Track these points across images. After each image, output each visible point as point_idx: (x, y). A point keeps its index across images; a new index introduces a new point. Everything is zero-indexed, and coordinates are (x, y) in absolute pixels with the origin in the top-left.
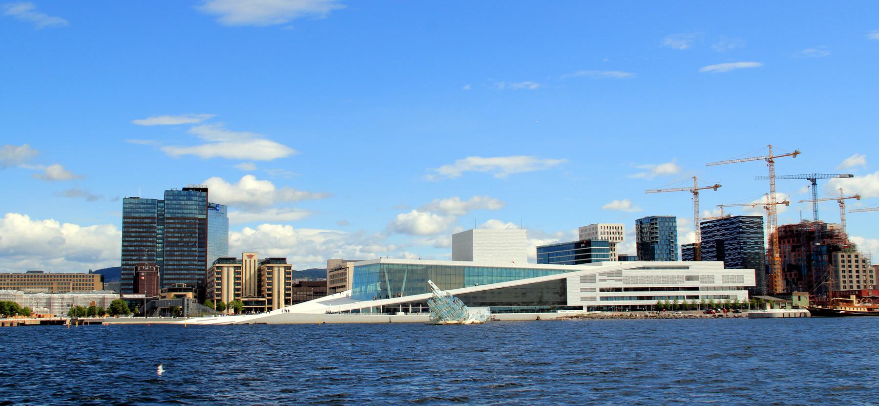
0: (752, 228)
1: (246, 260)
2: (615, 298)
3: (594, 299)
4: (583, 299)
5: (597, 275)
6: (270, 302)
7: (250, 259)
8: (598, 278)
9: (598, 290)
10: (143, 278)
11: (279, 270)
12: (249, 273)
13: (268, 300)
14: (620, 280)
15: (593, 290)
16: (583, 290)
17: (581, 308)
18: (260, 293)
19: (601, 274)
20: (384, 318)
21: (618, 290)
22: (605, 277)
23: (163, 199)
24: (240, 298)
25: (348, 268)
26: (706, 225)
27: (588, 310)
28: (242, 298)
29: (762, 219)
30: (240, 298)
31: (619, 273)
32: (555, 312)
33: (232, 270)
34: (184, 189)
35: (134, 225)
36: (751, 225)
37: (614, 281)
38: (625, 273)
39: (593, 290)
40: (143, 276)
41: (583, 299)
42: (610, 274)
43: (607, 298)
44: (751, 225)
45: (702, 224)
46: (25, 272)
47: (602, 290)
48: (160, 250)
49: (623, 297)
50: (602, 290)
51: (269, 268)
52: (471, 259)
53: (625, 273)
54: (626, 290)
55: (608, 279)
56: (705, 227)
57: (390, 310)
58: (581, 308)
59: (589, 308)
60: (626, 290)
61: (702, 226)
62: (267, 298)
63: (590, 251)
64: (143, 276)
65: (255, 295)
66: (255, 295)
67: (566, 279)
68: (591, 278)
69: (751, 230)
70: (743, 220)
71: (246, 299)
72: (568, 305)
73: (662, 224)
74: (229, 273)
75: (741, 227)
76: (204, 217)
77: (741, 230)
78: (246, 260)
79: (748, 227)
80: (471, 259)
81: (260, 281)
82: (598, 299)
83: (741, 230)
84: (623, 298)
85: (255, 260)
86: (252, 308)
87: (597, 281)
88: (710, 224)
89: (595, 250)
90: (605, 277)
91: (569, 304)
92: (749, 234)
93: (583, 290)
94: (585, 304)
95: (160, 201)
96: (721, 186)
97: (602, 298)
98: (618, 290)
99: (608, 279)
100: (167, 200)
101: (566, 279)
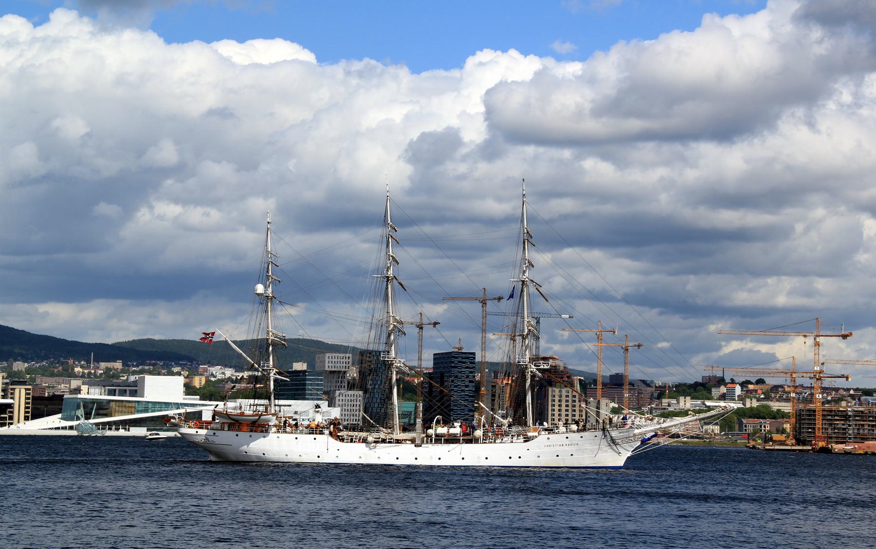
6: (11, 418)
11: (20, 391)
13: (9, 416)
36: (464, 360)
44: (464, 360)
45: (434, 355)
51: (12, 389)
52: (143, 396)
69: (463, 365)
70: (455, 356)
75: (453, 362)
77: (453, 365)
79: (460, 362)
83: (453, 365)
92: (461, 369)
96: (439, 323)
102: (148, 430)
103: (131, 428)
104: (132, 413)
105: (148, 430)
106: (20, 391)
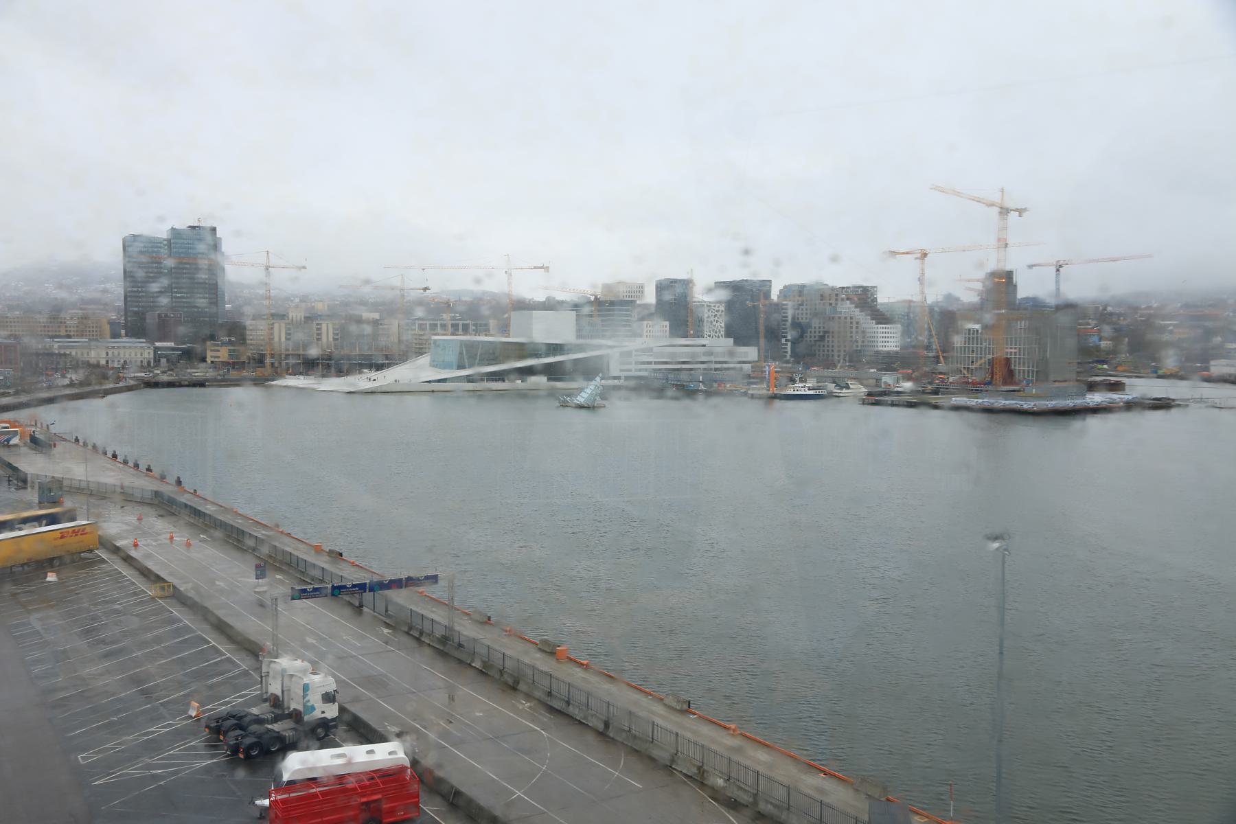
3: (630, 370)
4: (622, 370)
5: (634, 352)
8: (634, 353)
14: (651, 356)
19: (636, 351)
20: (470, 386)
21: (650, 363)
27: (625, 380)
31: (651, 350)
33: (283, 325)
42: (643, 350)
43: (640, 370)
51: (318, 324)
53: (655, 350)
54: (655, 363)
57: (469, 379)
59: (627, 378)
60: (655, 363)
63: (613, 310)
68: (629, 354)
89: (620, 310)
94: (623, 374)
95: (165, 240)
97: (636, 370)
100: (174, 239)
102: (549, 379)
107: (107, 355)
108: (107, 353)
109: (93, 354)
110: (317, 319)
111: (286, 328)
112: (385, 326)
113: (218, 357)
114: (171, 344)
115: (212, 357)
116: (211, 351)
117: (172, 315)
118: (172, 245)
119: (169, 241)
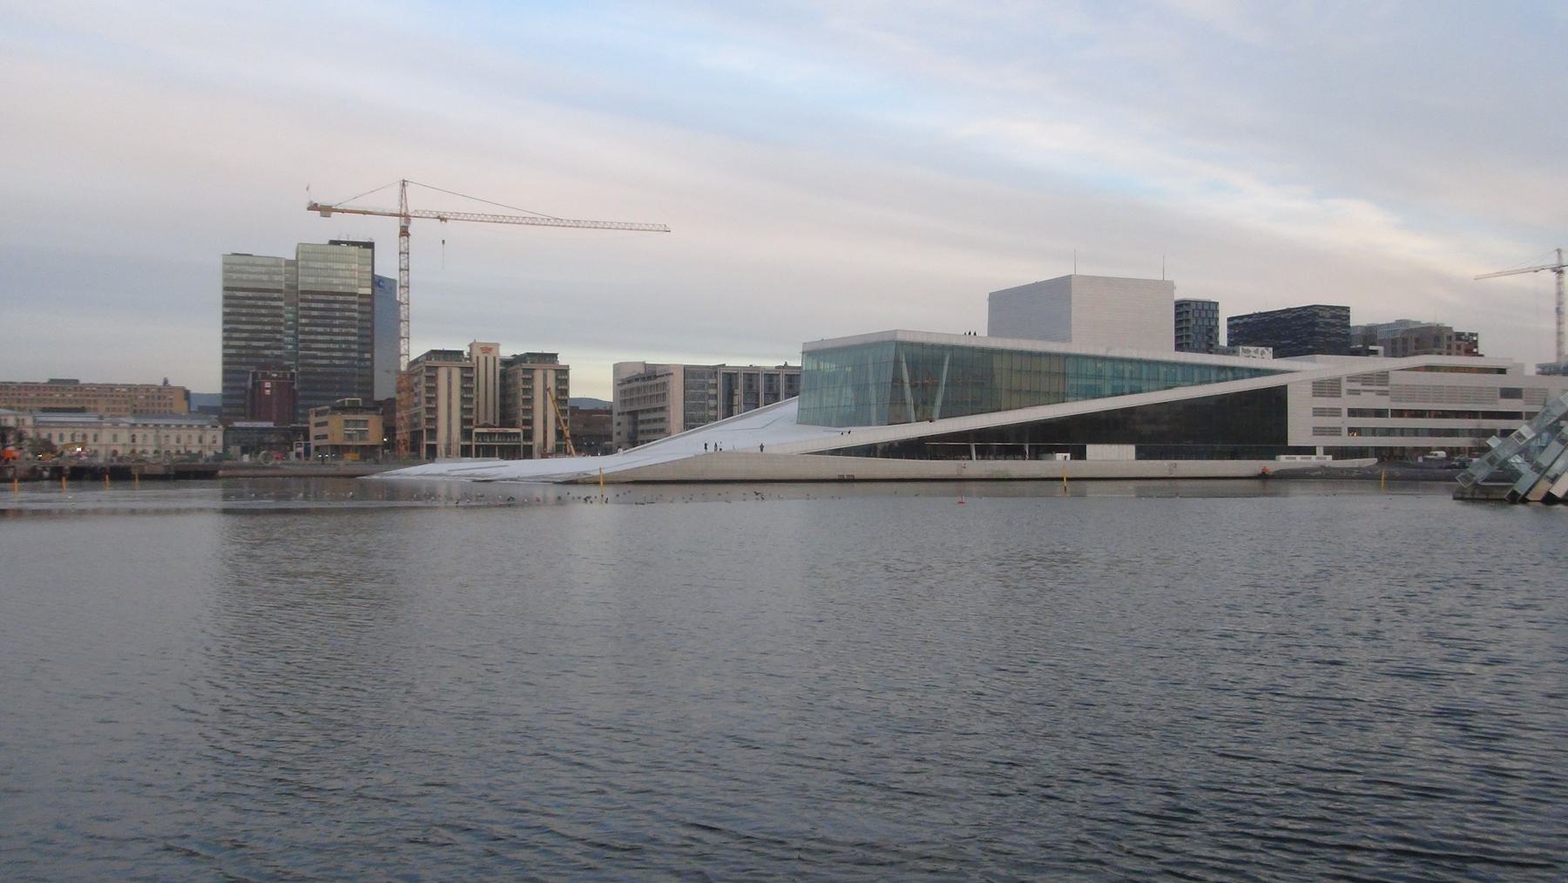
0: (1334, 325)
1: (478, 358)
2: (1374, 432)
3: (1335, 431)
4: (1319, 431)
5: (1344, 380)
7: (486, 355)
8: (1345, 386)
9: (1345, 412)
10: (268, 392)
11: (545, 376)
12: (487, 381)
13: (524, 431)
14: (1384, 393)
15: (1335, 412)
16: (1319, 412)
17: (1311, 451)
18: (506, 418)
19: (1351, 379)
21: (1379, 413)
22: (1357, 386)
23: (293, 257)
24: (472, 427)
25: (672, 374)
26: (1241, 322)
28: (477, 427)
29: (1349, 311)
30: (472, 427)
31: (1383, 377)
32: (1274, 459)
33: (456, 374)
34: (333, 243)
35: (248, 302)
37: (1374, 394)
38: (1395, 379)
39: (1335, 412)
40: (268, 389)
41: (1319, 431)
42: (1366, 379)
44: (1333, 321)
46: (46, 381)
47: (1353, 413)
48: (290, 347)
49: (1403, 429)
50: (1353, 413)
51: (526, 371)
53: (1395, 379)
54: (1399, 413)
55: (1365, 391)
56: (1237, 324)
58: (1311, 451)
59: (1328, 451)
60: (1399, 413)
61: (1232, 323)
62: (524, 427)
64: (268, 389)
65: (495, 423)
66: (495, 423)
67: (1285, 387)
71: (485, 430)
72: (1289, 445)
73: (1196, 315)
74: (449, 383)
76: (368, 291)
78: (478, 358)
79: (1327, 324)
80: (1067, 339)
81: (503, 396)
82: (1345, 431)
83: (1317, 329)
84: (1389, 432)
85: (495, 358)
86: (495, 446)
87: (1344, 392)
88: (1251, 320)
90: (1357, 386)
91: (1291, 443)
93: (1319, 412)
94: (1320, 442)
98: (1379, 413)
99: (1365, 391)
101: (1285, 387)
102: (1141, 455)
103: (1091, 449)
104: (1061, 398)
105: (1141, 455)
106: (545, 376)
107: (134, 441)
108: (133, 436)
109: (106, 437)
110: (525, 362)
111: (462, 377)
112: (658, 381)
113: (325, 437)
114: (271, 425)
115: (317, 437)
116: (317, 425)
117: (275, 375)
118: (300, 270)
119: (294, 263)
